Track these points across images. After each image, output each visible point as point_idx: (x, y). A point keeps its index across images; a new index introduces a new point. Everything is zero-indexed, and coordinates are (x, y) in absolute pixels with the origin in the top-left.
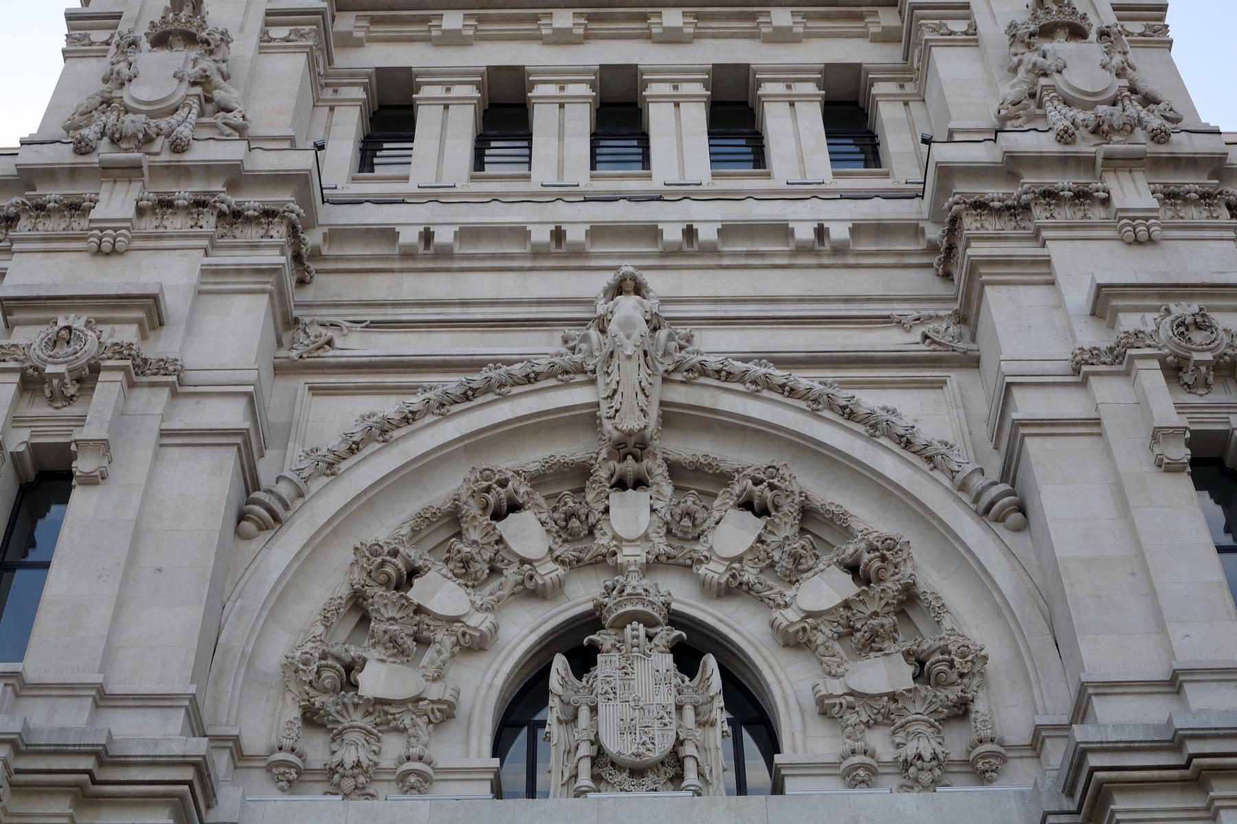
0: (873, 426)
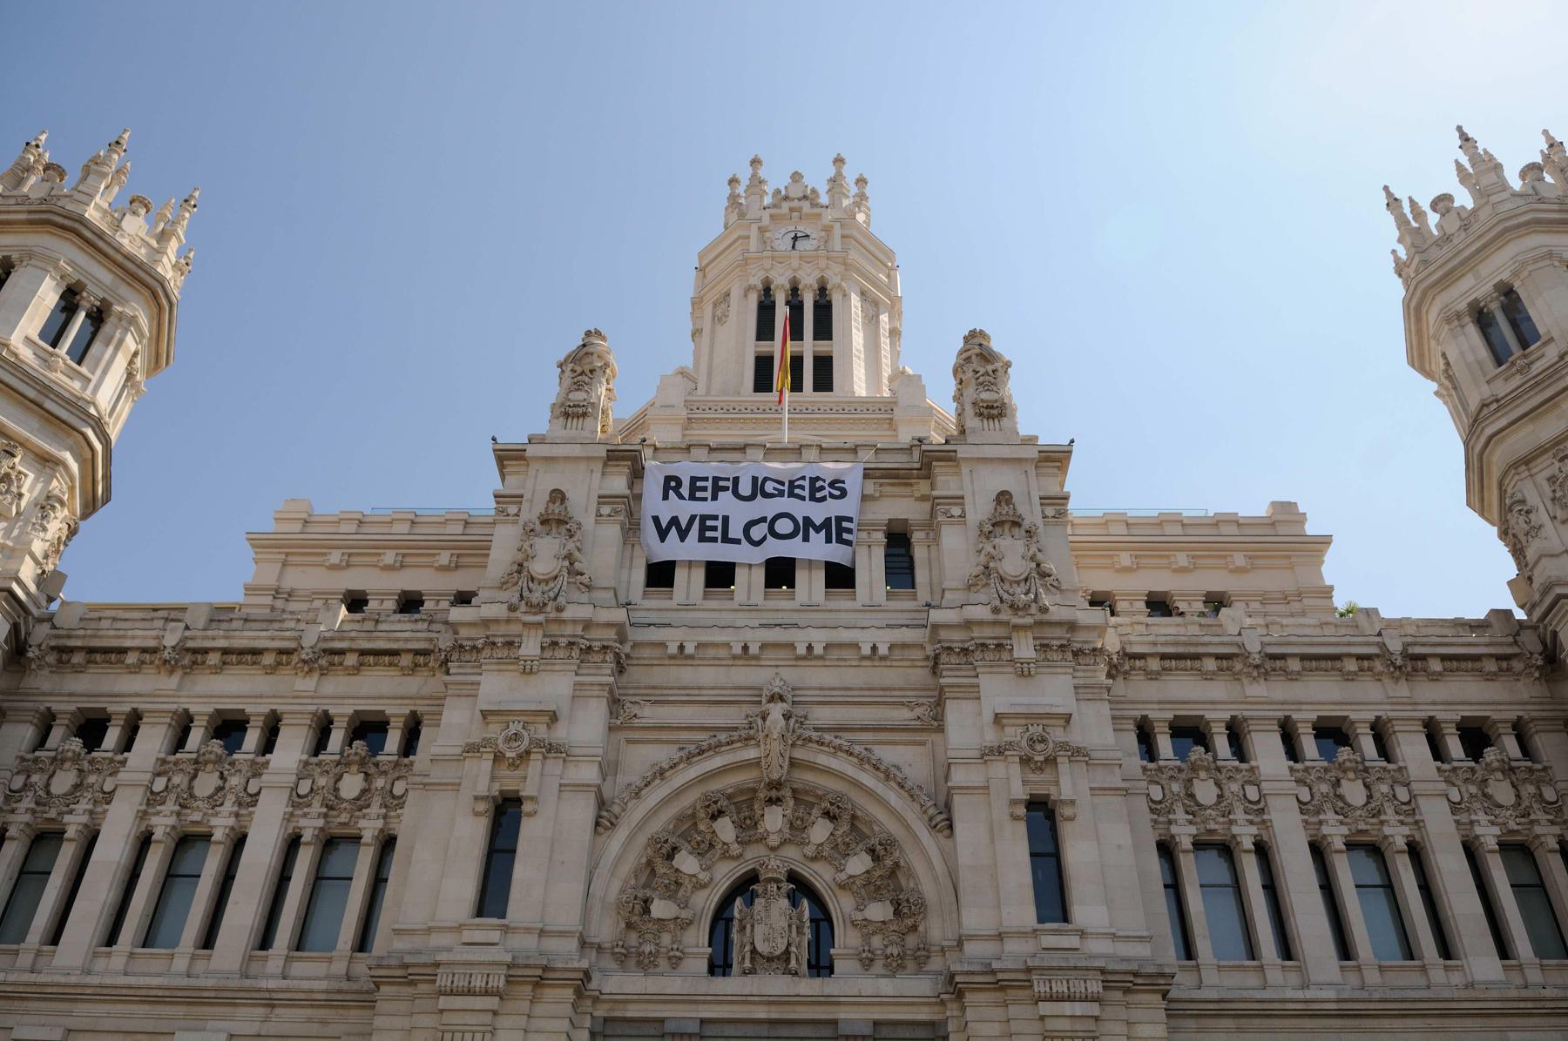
0: (887, 777)
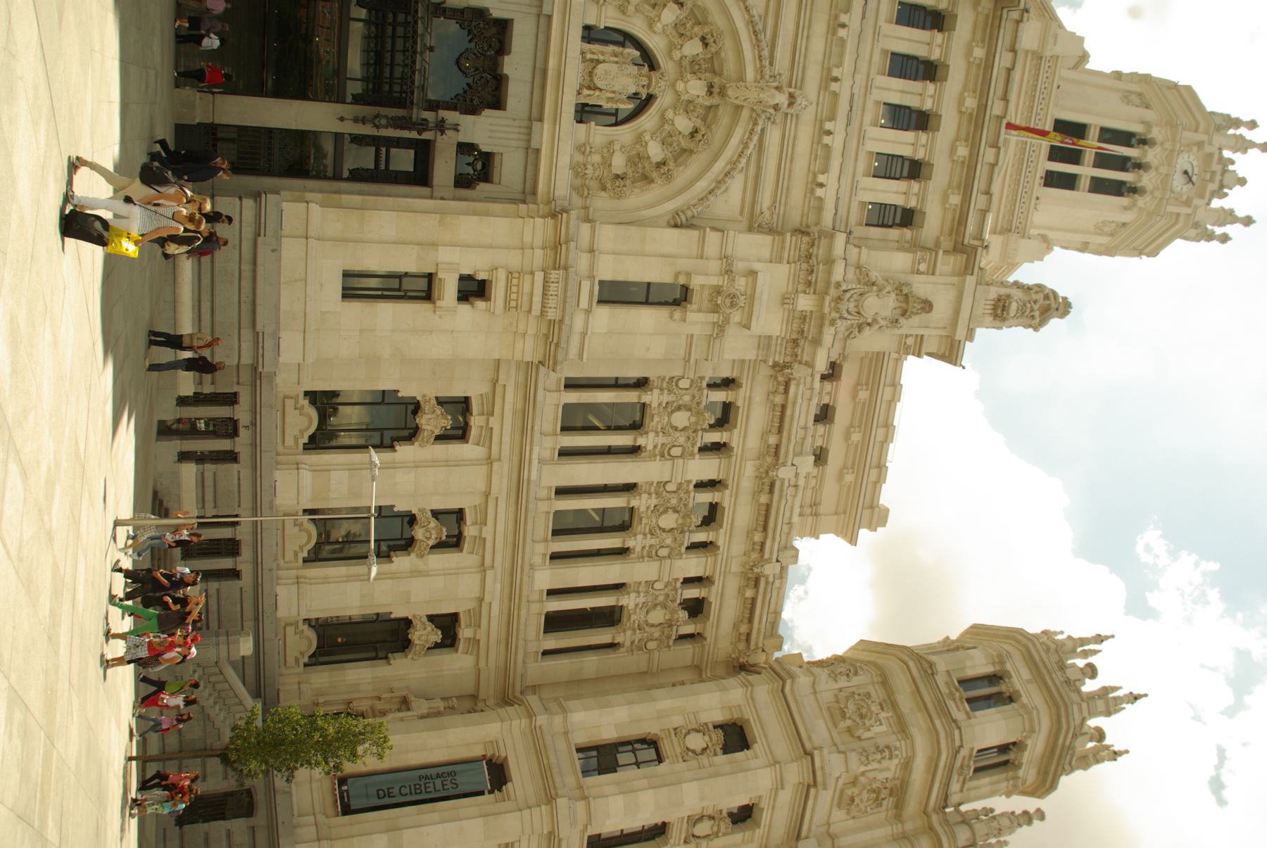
0: (719, 182)
